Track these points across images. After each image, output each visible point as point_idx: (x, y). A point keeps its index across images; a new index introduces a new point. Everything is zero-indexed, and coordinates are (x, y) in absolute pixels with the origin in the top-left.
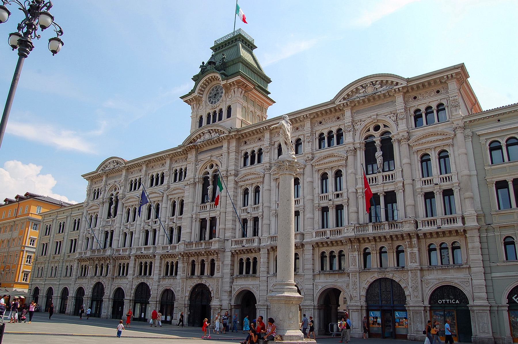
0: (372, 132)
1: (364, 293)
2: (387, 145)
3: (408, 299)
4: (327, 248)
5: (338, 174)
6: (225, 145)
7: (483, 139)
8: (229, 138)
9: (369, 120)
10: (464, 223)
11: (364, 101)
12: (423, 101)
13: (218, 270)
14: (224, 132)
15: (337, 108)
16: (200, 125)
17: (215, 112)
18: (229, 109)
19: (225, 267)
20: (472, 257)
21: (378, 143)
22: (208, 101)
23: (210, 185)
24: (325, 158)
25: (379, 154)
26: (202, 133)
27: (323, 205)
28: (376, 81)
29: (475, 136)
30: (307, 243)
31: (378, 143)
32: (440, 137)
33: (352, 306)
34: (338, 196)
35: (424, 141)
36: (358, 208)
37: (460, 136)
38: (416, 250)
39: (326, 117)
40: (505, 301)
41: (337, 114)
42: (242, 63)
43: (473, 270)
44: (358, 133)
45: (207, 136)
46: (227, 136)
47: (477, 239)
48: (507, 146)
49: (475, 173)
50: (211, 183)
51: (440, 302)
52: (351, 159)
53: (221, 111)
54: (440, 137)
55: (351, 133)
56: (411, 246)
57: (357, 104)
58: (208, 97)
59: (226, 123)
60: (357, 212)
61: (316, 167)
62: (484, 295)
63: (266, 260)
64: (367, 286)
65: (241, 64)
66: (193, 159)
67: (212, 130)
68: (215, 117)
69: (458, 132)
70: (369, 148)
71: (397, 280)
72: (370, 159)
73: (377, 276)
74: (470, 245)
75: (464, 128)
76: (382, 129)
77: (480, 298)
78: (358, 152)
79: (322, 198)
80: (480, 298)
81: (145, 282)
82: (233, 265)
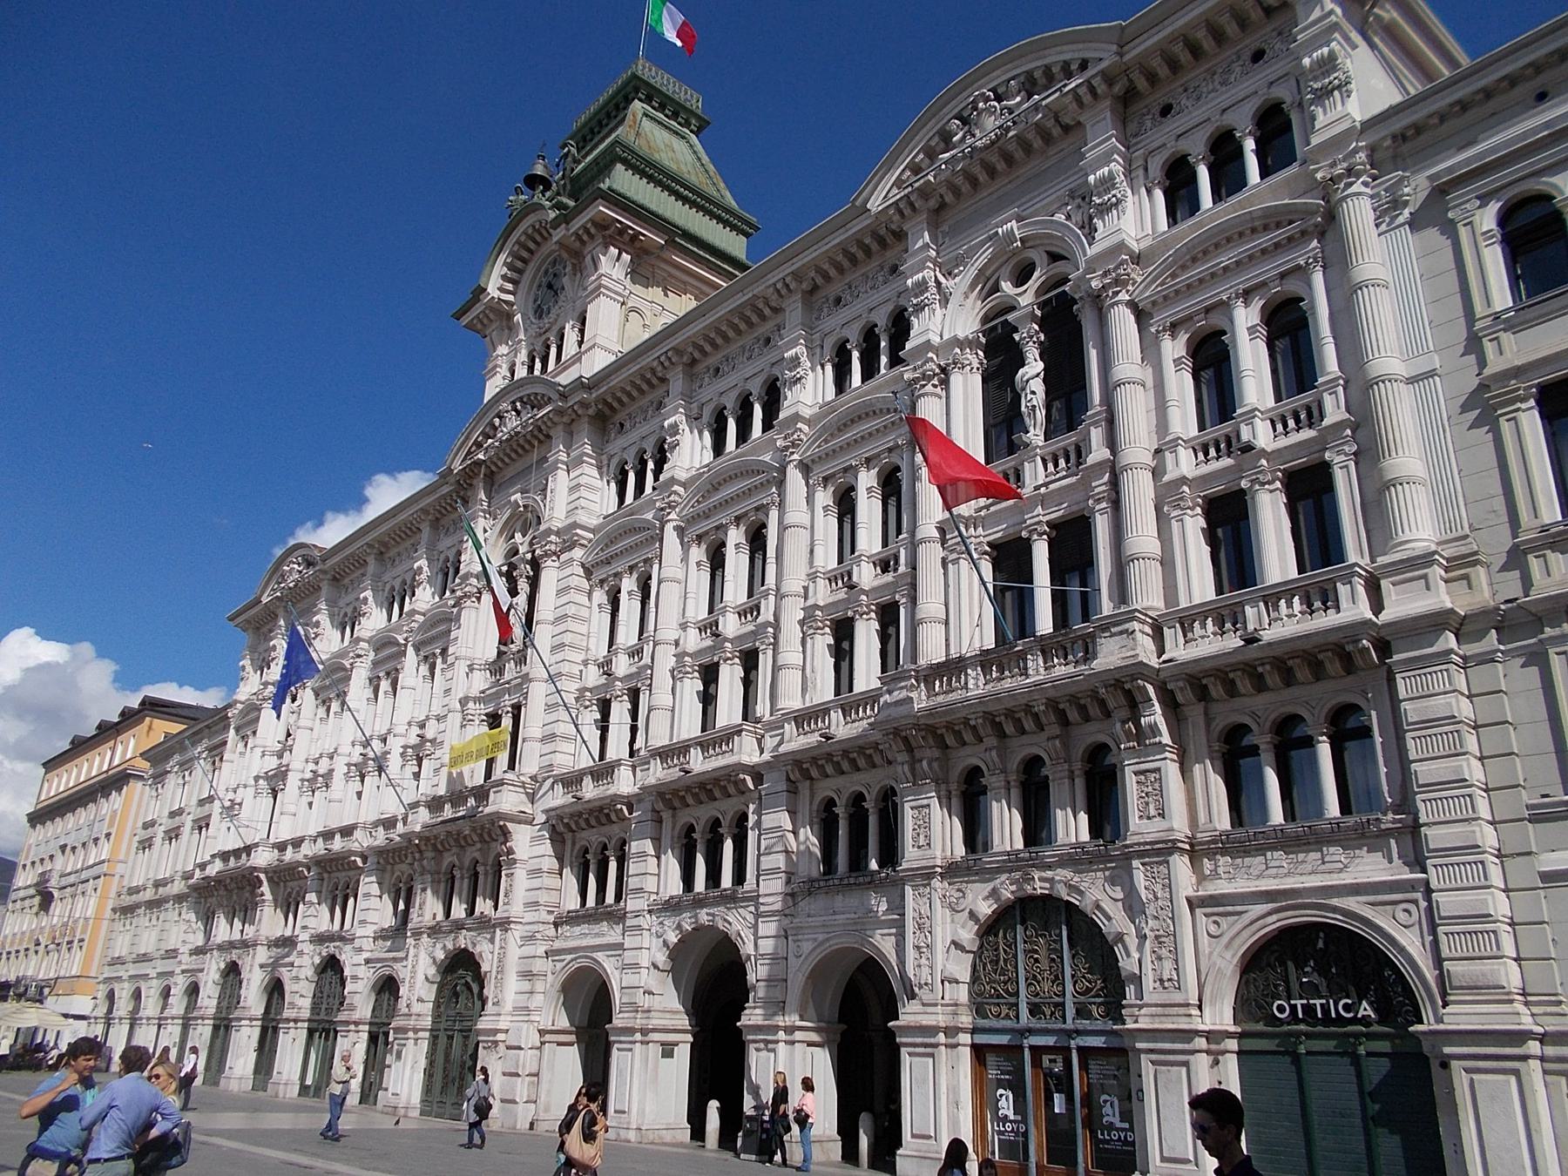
4: (840, 781)
8: (569, 422)
10: (1377, 605)
12: (1198, 114)
15: (883, 232)
19: (535, 878)
20: (1424, 772)
32: (1264, 240)
39: (853, 276)
41: (888, 254)
42: (625, 162)
46: (559, 412)
51: (1281, 1009)
54: (1264, 240)
57: (949, 198)
58: (531, 300)
65: (619, 167)
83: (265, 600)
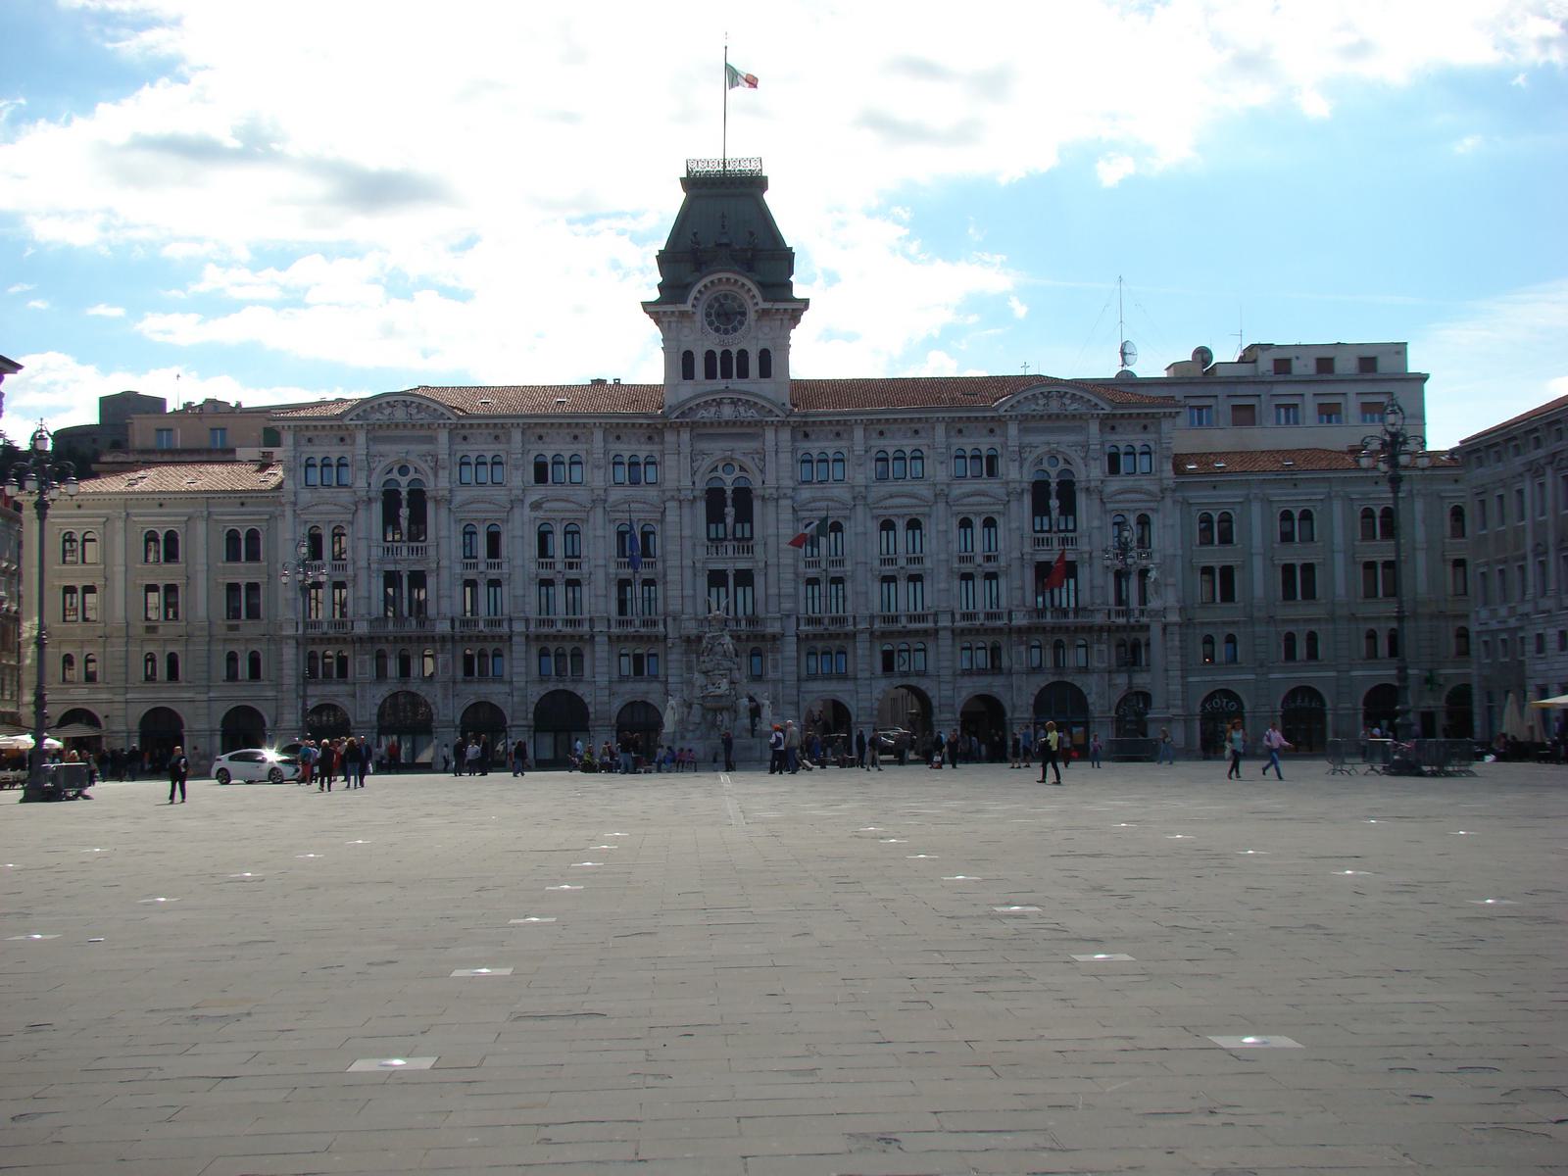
0: (1045, 466)
1: (1032, 701)
2: (1067, 491)
3: (1091, 708)
5: (990, 523)
6: (770, 434)
7: (1194, 508)
8: (778, 426)
9: (1045, 448)
11: (1042, 416)
13: (775, 667)
14: (771, 411)
16: (688, 373)
17: (726, 354)
18: (765, 357)
21: (1054, 485)
22: (706, 323)
23: (729, 506)
24: (969, 495)
25: (1054, 503)
26: (714, 400)
27: (963, 571)
28: (1066, 393)
29: (1186, 503)
30: (945, 628)
31: (1054, 485)
33: (1018, 719)
34: (988, 559)
35: (1121, 497)
36: (1023, 581)
37: (1168, 502)
38: (1104, 647)
40: (1198, 709)
43: (1171, 673)
44: (1026, 466)
45: (727, 412)
47: (1177, 638)
48: (1219, 522)
49: (1180, 552)
50: (729, 502)
52: (1014, 505)
53: (743, 355)
54: (1145, 497)
55: (1017, 464)
56: (1099, 641)
58: (704, 312)
59: (753, 384)
60: (1022, 588)
61: (954, 508)
62: (1180, 703)
63: (867, 653)
64: (1036, 692)
66: (686, 449)
67: (739, 400)
68: (725, 365)
69: (1168, 494)
70: (1040, 490)
71: (1078, 684)
72: (1040, 508)
73: (1052, 679)
74: (1169, 644)
75: (1174, 491)
76: (1062, 465)
77: (1174, 706)
78: (1025, 496)
79: (962, 559)
80: (1174, 706)
81: (570, 687)
82: (798, 658)
83: (347, 422)
